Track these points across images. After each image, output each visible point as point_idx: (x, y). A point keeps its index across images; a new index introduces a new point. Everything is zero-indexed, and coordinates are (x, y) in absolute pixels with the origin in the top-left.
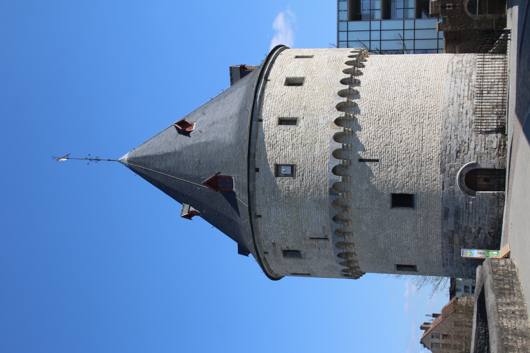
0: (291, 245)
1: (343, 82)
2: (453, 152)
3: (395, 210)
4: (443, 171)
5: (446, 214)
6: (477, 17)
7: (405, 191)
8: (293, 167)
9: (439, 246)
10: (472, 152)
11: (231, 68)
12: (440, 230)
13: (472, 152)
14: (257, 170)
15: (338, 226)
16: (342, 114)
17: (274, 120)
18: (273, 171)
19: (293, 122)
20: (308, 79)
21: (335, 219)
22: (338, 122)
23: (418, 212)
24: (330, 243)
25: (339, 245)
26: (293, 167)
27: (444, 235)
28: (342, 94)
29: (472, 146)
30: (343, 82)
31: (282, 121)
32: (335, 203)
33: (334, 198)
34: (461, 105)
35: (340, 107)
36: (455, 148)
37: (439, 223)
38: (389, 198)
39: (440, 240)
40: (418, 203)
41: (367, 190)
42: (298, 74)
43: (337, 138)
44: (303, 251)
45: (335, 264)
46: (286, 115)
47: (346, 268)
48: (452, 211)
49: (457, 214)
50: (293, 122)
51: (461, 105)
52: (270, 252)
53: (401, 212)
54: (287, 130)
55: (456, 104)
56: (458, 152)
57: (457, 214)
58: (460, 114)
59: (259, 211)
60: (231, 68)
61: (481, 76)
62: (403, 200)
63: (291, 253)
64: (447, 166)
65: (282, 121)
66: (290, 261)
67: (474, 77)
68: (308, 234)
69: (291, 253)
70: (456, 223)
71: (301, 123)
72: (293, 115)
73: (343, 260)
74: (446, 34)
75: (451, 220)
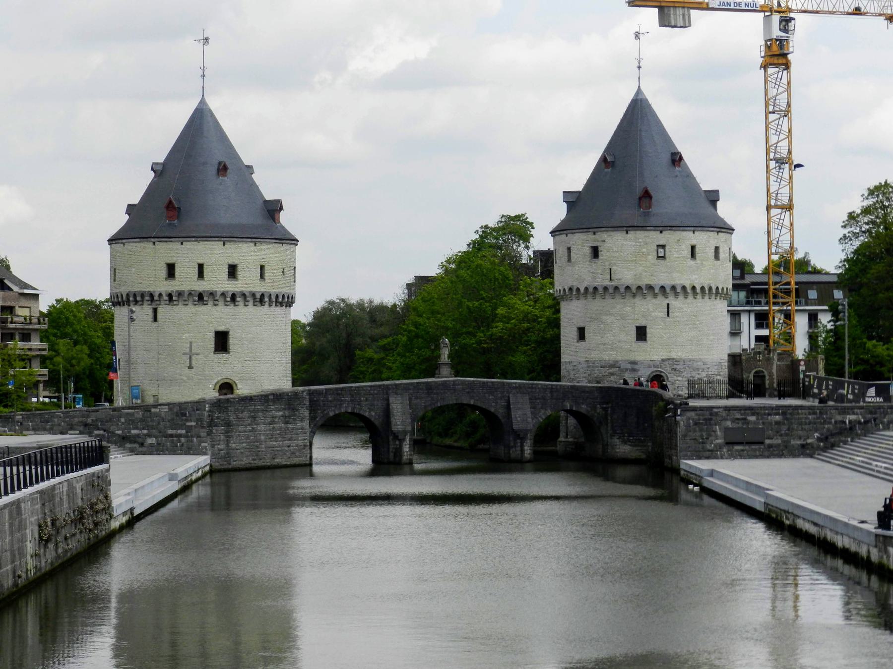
0: (603, 254)
1: (717, 288)
2: (675, 366)
3: (635, 329)
4: (663, 360)
5: (634, 363)
6: (751, 377)
7: (648, 336)
8: (664, 257)
9: (607, 358)
10: (676, 378)
11: (718, 191)
12: (620, 358)
13: (676, 378)
14: (661, 232)
15: (622, 290)
16: (698, 290)
17: (694, 242)
18: (661, 243)
19: (693, 255)
20: (719, 262)
21: (628, 288)
22: (694, 288)
23: (634, 345)
24: (607, 283)
25: (606, 289)
26: (664, 257)
27: (617, 362)
28: (710, 289)
29: (680, 378)
30: (717, 288)
31: (693, 248)
32: (639, 288)
33: (644, 287)
34: (703, 370)
35: (703, 288)
36: (678, 367)
37: (627, 358)
38: (643, 324)
39: (612, 358)
40: (641, 344)
41: (648, 310)
42: (722, 255)
43: (684, 288)
44: (599, 262)
45: (585, 284)
46: (697, 250)
47: (582, 290)
48: (636, 367)
49: (634, 370)
50: (693, 255)
51: (703, 370)
52: (597, 236)
53: (633, 333)
54: (687, 252)
55: (704, 366)
56: (675, 370)
57: (634, 370)
58: (698, 369)
59: (632, 234)
60: (718, 191)
61: (719, 382)
62: (641, 333)
63: (595, 252)
64: (667, 363)
65: (693, 248)
66: (587, 251)
67: (719, 377)
68: (614, 268)
69: (595, 252)
70: (627, 370)
71: (692, 263)
72: (698, 255)
73: (591, 290)
74: (740, 355)
75: (629, 366)
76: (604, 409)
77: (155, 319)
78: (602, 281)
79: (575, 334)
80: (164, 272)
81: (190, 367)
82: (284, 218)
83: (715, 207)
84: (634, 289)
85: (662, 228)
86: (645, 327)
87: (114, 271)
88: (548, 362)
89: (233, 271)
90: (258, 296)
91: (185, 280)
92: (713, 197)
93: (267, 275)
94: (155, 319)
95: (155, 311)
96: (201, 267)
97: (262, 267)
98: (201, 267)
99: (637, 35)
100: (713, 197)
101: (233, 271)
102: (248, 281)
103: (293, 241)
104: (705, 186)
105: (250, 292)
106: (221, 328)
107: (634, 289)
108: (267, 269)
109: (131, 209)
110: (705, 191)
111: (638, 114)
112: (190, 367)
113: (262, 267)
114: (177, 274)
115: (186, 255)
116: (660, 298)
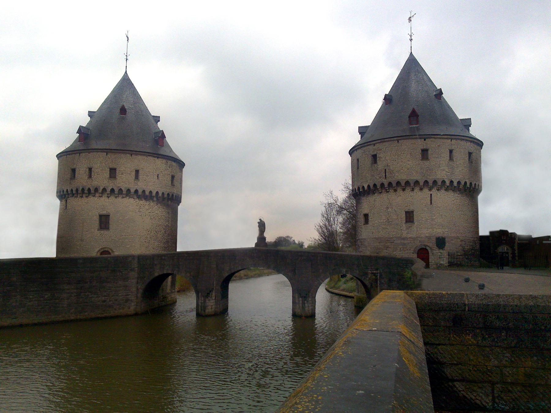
7: (415, 218)
40: (409, 224)
62: (410, 217)
76: (374, 274)
83: (469, 130)
84: (403, 184)
85: (425, 137)
89: (113, 172)
92: (467, 123)
93: (140, 177)
95: (66, 201)
97: (137, 172)
98: (90, 169)
99: (410, 20)
100: (467, 123)
101: (113, 172)
102: (125, 180)
104: (460, 116)
105: (125, 188)
106: (104, 212)
107: (403, 184)
108: (140, 172)
110: (461, 120)
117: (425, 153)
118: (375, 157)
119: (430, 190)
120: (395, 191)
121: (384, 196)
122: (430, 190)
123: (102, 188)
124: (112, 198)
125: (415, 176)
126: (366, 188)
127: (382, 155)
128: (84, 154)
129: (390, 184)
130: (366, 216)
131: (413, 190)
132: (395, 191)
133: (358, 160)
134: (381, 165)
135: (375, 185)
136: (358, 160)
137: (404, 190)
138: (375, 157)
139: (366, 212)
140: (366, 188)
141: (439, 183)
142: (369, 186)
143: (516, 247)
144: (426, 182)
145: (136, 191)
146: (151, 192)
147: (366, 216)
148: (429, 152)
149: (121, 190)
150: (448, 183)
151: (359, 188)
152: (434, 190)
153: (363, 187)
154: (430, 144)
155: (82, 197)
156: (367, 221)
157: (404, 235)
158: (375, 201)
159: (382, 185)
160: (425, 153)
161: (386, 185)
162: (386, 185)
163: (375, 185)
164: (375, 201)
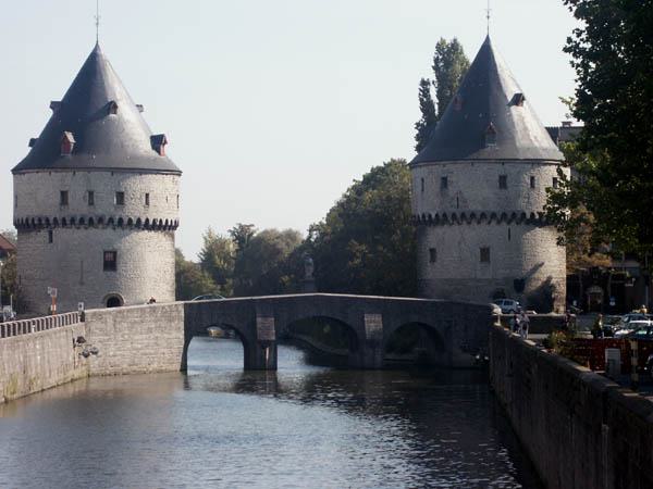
62: (485, 254)
77: (51, 241)
78: (450, 210)
79: (429, 256)
80: (58, 199)
81: (82, 283)
82: (167, 149)
84: (478, 216)
86: (488, 249)
87: (16, 197)
88: (412, 283)
90: (143, 220)
91: (77, 206)
94: (51, 241)
95: (51, 233)
96: (91, 194)
98: (91, 194)
103: (179, 173)
109: (32, 142)
111: (91, 72)
112: (82, 283)
113: (147, 195)
114: (70, 200)
115: (76, 184)
116: (504, 224)
117: (503, 181)
118: (444, 180)
119: (509, 223)
120: (469, 223)
121: (456, 227)
122: (509, 223)
123: (107, 218)
124: (119, 230)
125: (492, 208)
126: (433, 216)
127: (454, 179)
128: (81, 173)
129: (463, 215)
130: (433, 251)
131: (489, 223)
132: (469, 223)
133: (423, 180)
134: (451, 191)
135: (445, 215)
136: (423, 180)
137: (479, 223)
138: (444, 180)
139: (432, 247)
140: (433, 216)
141: (519, 216)
142: (437, 215)
143: (609, 289)
144: (504, 215)
145: (147, 220)
146: (161, 221)
147: (433, 251)
148: (509, 179)
149: (130, 220)
150: (528, 216)
151: (424, 216)
152: (513, 223)
153: (430, 216)
154: (509, 169)
155: (78, 228)
156: (433, 259)
157: (478, 277)
158: (444, 233)
159: (454, 215)
160: (503, 181)
161: (458, 216)
162: (458, 216)
163: (445, 215)
164: (444, 233)
